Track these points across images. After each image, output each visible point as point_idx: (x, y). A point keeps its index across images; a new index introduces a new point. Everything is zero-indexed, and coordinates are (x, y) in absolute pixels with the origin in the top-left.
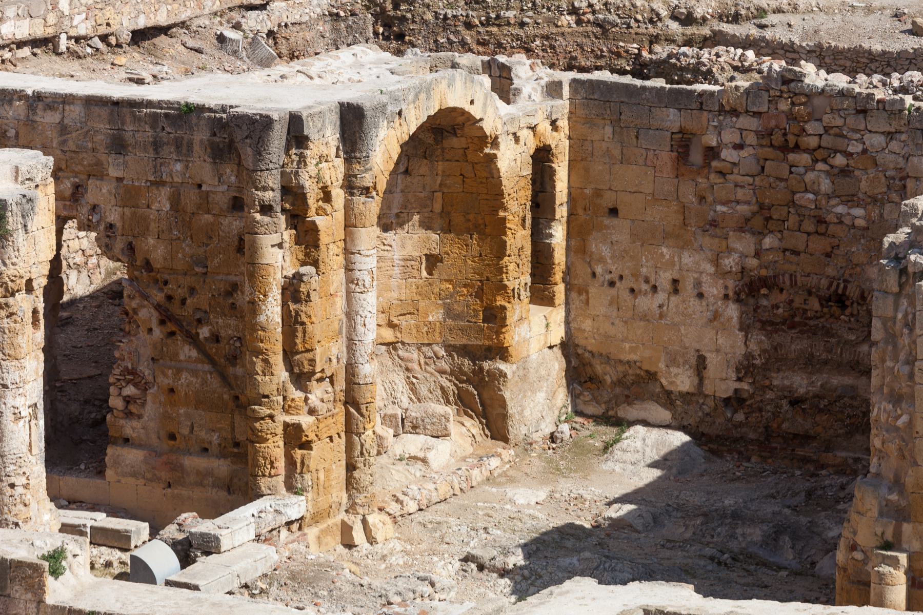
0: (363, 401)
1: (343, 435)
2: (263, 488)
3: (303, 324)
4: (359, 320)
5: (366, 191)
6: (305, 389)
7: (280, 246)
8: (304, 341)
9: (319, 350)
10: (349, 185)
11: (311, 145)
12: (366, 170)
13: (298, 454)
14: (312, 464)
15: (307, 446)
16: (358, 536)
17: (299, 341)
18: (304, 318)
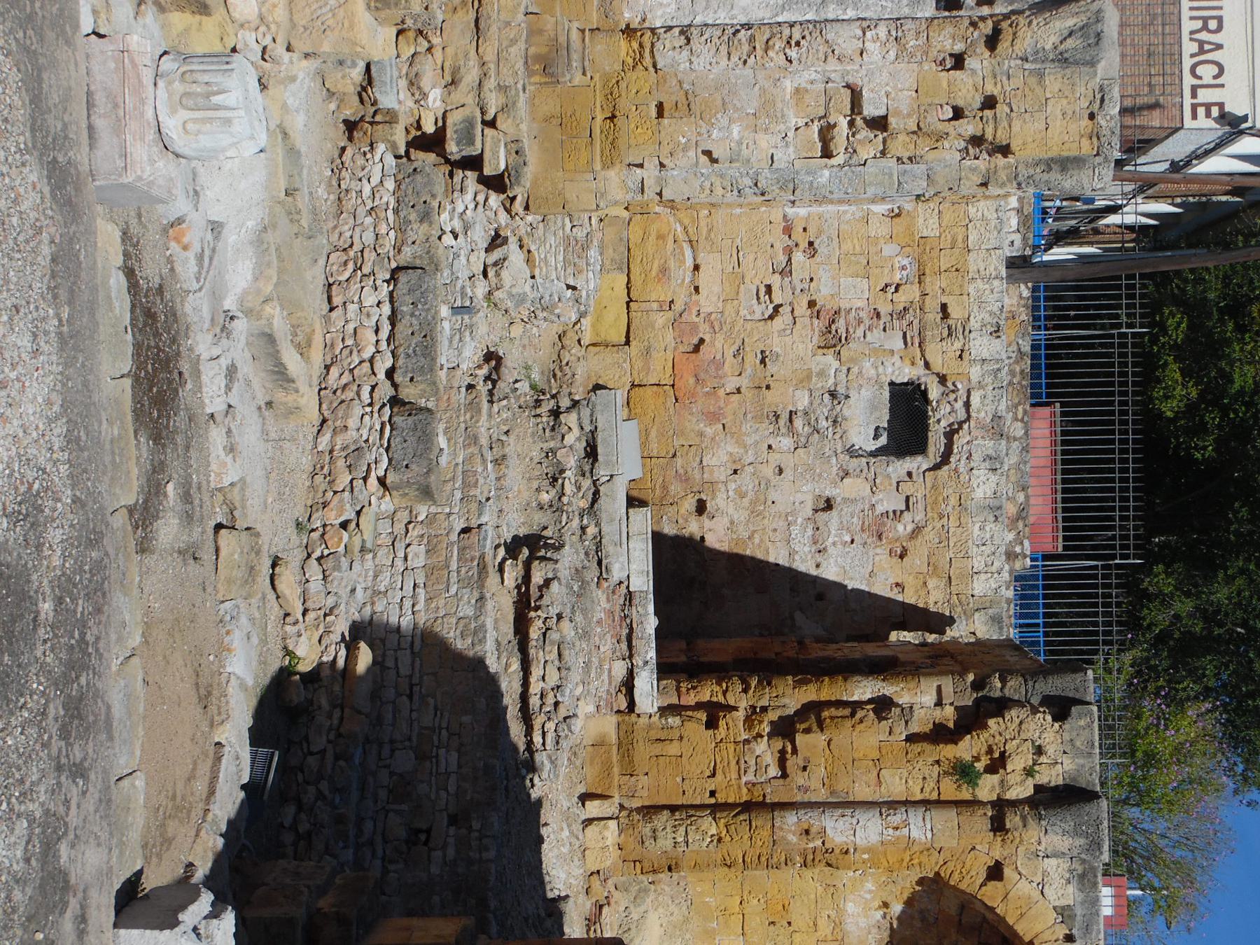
0: (753, 815)
1: (713, 801)
2: (665, 682)
3: (853, 715)
4: (848, 812)
5: (998, 826)
6: (770, 736)
7: (939, 703)
8: (832, 718)
9: (818, 739)
10: (1001, 807)
11: (1057, 725)
12: (1024, 818)
13: (703, 716)
14: (690, 726)
15: (712, 724)
16: (594, 808)
17: (833, 711)
18: (860, 714)
